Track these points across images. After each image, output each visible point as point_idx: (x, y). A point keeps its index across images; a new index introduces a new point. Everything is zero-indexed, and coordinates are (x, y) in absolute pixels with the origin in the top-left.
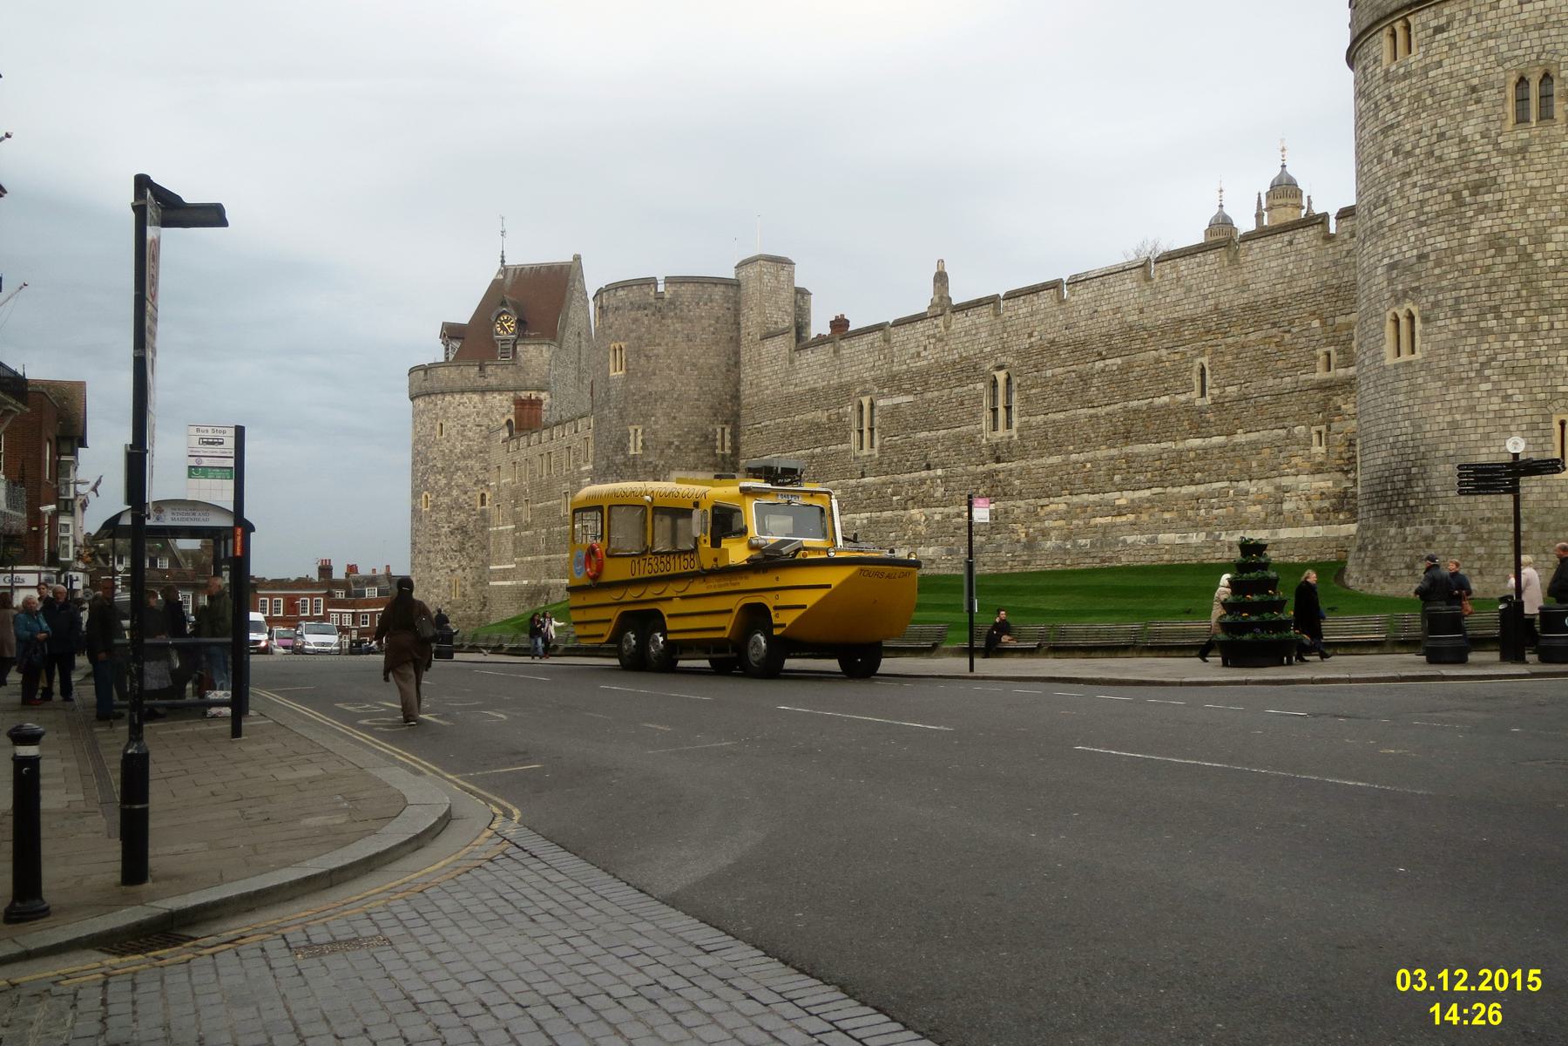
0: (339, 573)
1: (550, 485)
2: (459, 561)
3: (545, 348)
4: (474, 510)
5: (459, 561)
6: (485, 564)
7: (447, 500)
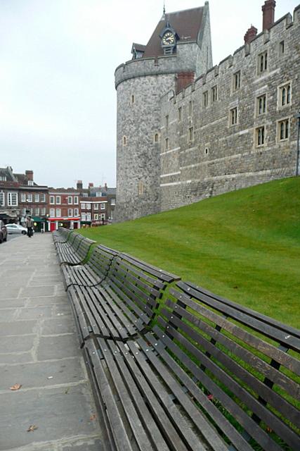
0: (85, 187)
1: (213, 109)
2: (143, 173)
3: (193, 45)
4: (151, 144)
5: (143, 173)
6: (158, 174)
7: (136, 139)
